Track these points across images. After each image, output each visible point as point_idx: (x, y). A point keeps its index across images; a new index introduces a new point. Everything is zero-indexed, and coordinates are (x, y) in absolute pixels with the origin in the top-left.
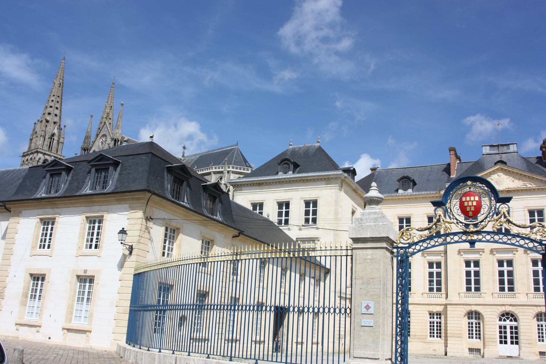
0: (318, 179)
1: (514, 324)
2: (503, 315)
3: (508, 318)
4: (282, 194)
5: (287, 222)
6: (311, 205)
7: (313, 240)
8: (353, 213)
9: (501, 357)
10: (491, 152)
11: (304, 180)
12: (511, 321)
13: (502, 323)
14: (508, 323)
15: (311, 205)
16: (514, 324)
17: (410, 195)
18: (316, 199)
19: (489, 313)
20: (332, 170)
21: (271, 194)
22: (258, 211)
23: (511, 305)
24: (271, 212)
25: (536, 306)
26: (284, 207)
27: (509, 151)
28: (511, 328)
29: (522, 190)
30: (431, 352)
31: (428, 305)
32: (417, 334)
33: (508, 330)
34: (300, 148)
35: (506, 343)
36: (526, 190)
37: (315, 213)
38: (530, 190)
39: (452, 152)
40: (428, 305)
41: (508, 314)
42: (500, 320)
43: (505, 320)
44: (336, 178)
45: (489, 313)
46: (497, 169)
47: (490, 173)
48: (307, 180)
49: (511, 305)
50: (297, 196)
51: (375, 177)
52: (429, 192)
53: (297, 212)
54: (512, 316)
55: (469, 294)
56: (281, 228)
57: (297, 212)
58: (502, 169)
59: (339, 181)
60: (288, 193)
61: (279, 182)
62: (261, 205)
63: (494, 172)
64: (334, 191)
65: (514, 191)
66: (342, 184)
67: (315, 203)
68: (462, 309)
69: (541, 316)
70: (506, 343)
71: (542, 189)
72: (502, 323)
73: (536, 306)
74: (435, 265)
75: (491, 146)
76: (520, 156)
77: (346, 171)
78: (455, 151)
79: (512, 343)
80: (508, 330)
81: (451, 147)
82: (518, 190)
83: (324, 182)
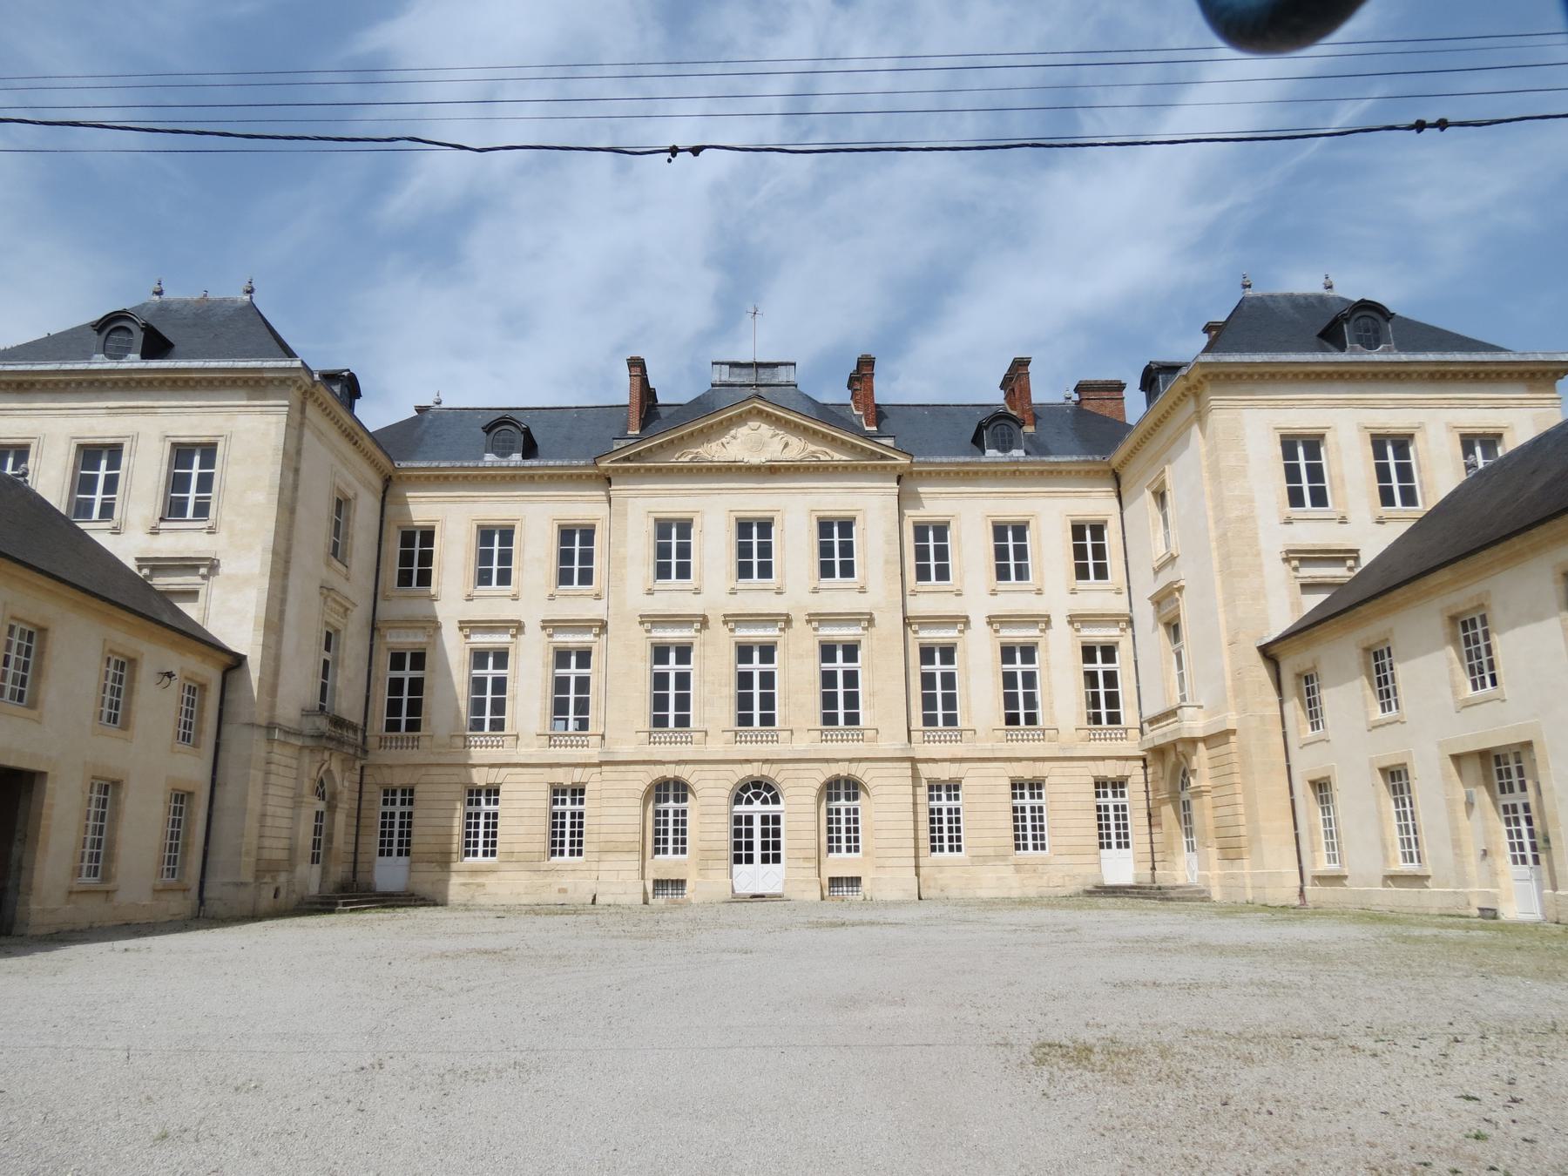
0: (223, 381)
1: (771, 809)
2: (745, 789)
3: (757, 796)
4: (97, 420)
5: (107, 511)
6: (197, 459)
7: (187, 565)
8: (341, 505)
9: (737, 899)
10: (733, 380)
11: (175, 381)
12: (765, 801)
13: (742, 809)
14: (757, 809)
15: (197, 459)
16: (771, 809)
17: (515, 468)
18: (213, 440)
19: (711, 783)
20: (270, 355)
21: (61, 420)
22: (9, 471)
23: (766, 761)
24: (50, 480)
25: (827, 761)
26: (104, 463)
27: (775, 381)
28: (765, 820)
29: (807, 468)
30: (552, 897)
31: (551, 765)
32: (516, 848)
33: (757, 827)
34: (187, 303)
35: (750, 860)
36: (816, 468)
37: (206, 483)
38: (826, 468)
39: (637, 371)
40: (551, 765)
41: (757, 784)
42: (738, 800)
43: (749, 802)
44: (283, 381)
45: (711, 783)
46: (749, 412)
47: (730, 418)
48: (186, 381)
49: (766, 761)
50: (147, 431)
51: (426, 424)
52: (566, 463)
53: (144, 475)
54: (769, 788)
55: (660, 734)
56: (82, 526)
57: (144, 475)
58: (760, 412)
59: (295, 393)
60: (122, 418)
61: (91, 383)
62: (22, 452)
63: (741, 420)
64: (273, 419)
65: (788, 468)
66: (303, 404)
67: (208, 451)
68: (642, 775)
69: (838, 788)
70: (750, 860)
71: (855, 468)
72: (742, 809)
73: (827, 761)
74: (573, 659)
75: (733, 365)
76: (801, 394)
77: (330, 377)
78: (644, 370)
79: (765, 859)
80: (757, 827)
81: (635, 355)
82: (797, 469)
83: (243, 393)
